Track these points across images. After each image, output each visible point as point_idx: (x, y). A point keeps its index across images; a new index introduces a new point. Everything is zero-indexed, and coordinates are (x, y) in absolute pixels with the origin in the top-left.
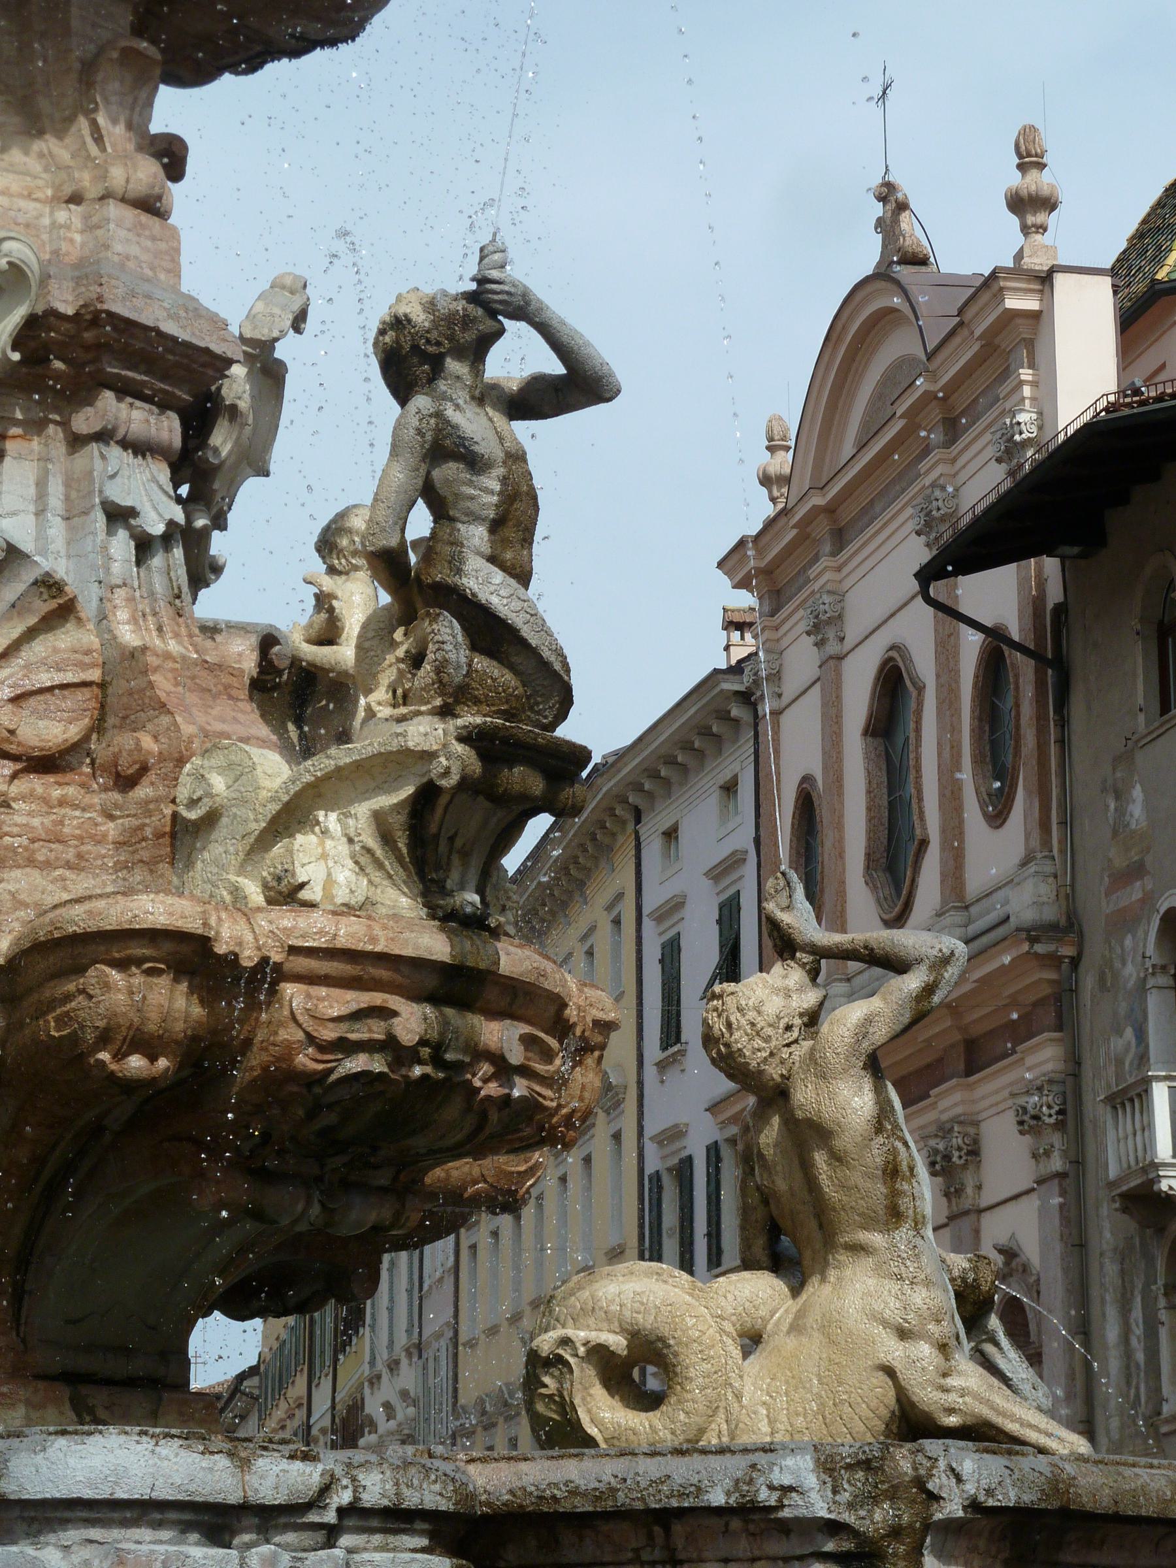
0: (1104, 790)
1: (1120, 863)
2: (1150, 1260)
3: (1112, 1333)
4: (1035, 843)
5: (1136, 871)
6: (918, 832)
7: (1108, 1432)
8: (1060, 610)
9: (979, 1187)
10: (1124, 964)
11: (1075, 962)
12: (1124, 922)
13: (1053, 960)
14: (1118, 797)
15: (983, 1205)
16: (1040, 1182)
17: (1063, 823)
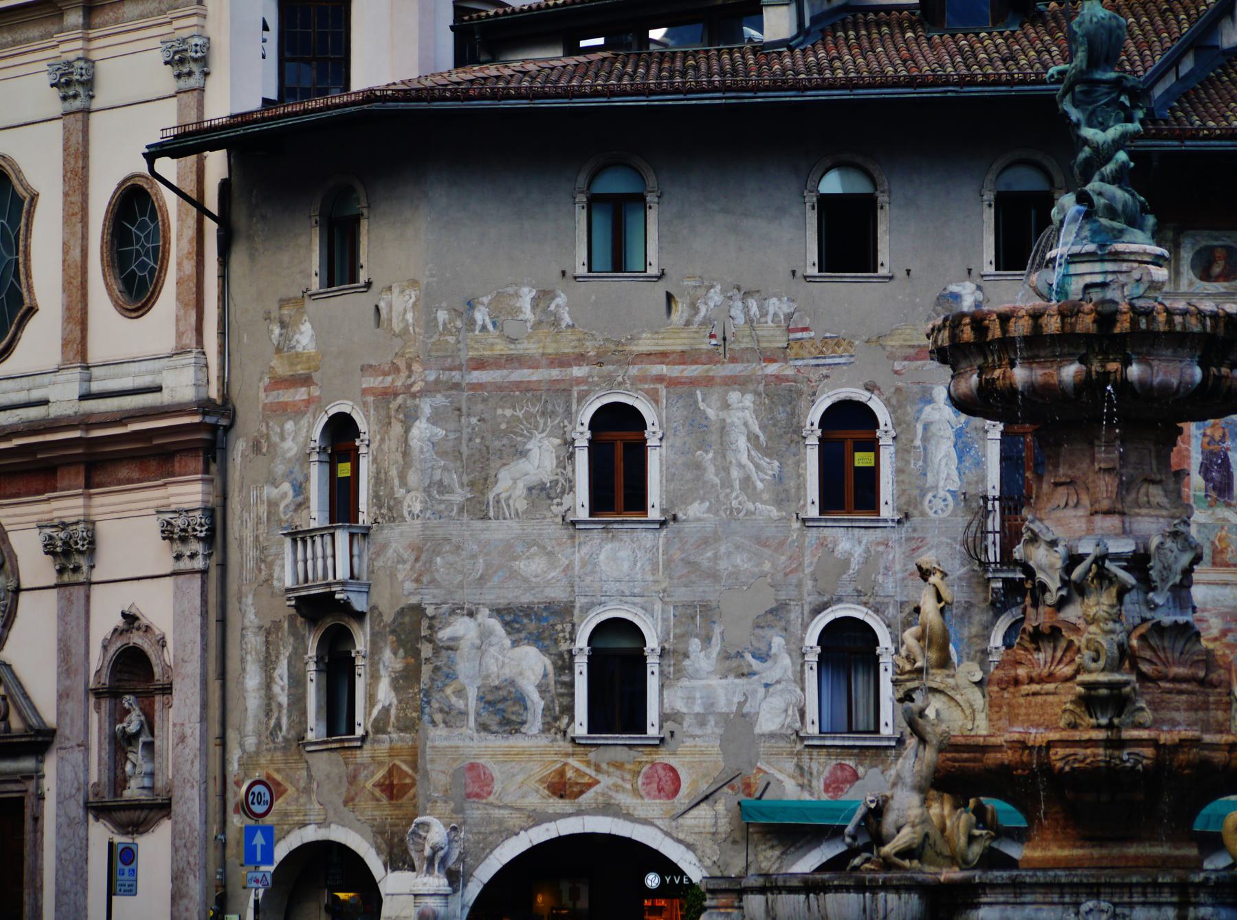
0: (268, 317)
1: (282, 370)
2: (300, 640)
3: (252, 680)
4: (190, 339)
5: (306, 381)
6: (27, 301)
7: (241, 745)
8: (225, 187)
9: (92, 567)
10: (283, 438)
11: (227, 429)
12: (282, 411)
13: (214, 428)
14: (283, 325)
15: (94, 579)
16: (174, 574)
17: (223, 332)
